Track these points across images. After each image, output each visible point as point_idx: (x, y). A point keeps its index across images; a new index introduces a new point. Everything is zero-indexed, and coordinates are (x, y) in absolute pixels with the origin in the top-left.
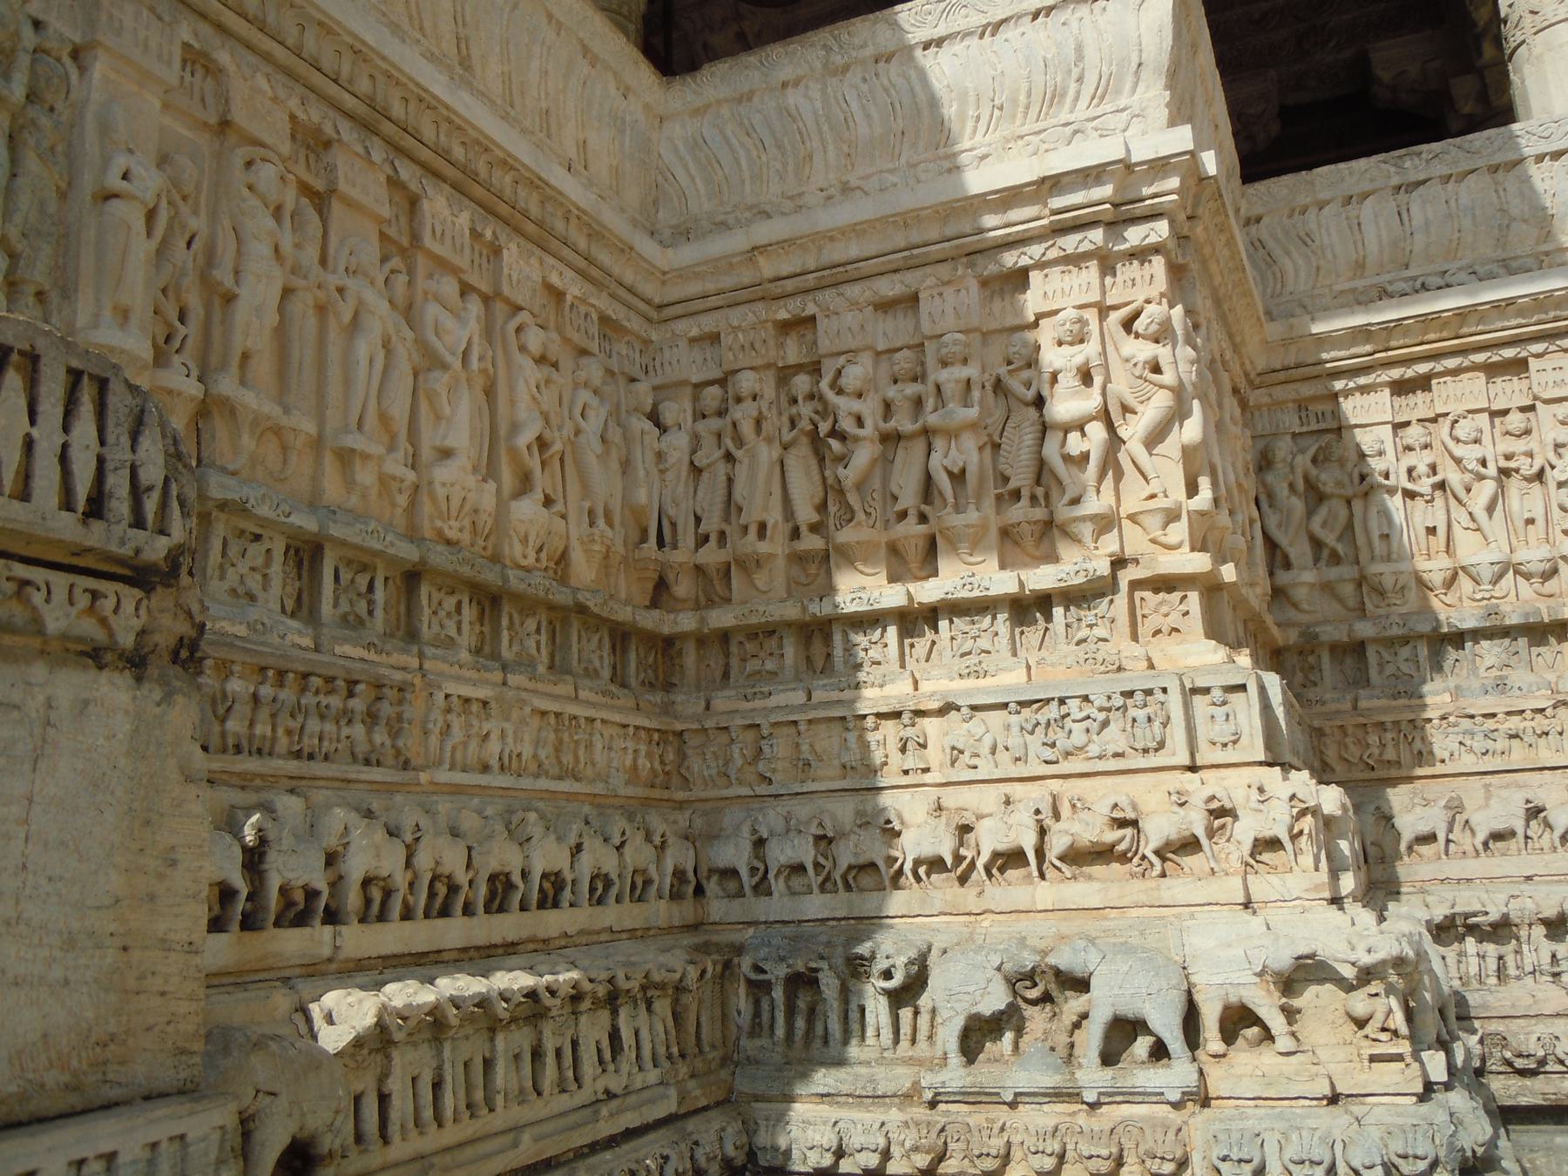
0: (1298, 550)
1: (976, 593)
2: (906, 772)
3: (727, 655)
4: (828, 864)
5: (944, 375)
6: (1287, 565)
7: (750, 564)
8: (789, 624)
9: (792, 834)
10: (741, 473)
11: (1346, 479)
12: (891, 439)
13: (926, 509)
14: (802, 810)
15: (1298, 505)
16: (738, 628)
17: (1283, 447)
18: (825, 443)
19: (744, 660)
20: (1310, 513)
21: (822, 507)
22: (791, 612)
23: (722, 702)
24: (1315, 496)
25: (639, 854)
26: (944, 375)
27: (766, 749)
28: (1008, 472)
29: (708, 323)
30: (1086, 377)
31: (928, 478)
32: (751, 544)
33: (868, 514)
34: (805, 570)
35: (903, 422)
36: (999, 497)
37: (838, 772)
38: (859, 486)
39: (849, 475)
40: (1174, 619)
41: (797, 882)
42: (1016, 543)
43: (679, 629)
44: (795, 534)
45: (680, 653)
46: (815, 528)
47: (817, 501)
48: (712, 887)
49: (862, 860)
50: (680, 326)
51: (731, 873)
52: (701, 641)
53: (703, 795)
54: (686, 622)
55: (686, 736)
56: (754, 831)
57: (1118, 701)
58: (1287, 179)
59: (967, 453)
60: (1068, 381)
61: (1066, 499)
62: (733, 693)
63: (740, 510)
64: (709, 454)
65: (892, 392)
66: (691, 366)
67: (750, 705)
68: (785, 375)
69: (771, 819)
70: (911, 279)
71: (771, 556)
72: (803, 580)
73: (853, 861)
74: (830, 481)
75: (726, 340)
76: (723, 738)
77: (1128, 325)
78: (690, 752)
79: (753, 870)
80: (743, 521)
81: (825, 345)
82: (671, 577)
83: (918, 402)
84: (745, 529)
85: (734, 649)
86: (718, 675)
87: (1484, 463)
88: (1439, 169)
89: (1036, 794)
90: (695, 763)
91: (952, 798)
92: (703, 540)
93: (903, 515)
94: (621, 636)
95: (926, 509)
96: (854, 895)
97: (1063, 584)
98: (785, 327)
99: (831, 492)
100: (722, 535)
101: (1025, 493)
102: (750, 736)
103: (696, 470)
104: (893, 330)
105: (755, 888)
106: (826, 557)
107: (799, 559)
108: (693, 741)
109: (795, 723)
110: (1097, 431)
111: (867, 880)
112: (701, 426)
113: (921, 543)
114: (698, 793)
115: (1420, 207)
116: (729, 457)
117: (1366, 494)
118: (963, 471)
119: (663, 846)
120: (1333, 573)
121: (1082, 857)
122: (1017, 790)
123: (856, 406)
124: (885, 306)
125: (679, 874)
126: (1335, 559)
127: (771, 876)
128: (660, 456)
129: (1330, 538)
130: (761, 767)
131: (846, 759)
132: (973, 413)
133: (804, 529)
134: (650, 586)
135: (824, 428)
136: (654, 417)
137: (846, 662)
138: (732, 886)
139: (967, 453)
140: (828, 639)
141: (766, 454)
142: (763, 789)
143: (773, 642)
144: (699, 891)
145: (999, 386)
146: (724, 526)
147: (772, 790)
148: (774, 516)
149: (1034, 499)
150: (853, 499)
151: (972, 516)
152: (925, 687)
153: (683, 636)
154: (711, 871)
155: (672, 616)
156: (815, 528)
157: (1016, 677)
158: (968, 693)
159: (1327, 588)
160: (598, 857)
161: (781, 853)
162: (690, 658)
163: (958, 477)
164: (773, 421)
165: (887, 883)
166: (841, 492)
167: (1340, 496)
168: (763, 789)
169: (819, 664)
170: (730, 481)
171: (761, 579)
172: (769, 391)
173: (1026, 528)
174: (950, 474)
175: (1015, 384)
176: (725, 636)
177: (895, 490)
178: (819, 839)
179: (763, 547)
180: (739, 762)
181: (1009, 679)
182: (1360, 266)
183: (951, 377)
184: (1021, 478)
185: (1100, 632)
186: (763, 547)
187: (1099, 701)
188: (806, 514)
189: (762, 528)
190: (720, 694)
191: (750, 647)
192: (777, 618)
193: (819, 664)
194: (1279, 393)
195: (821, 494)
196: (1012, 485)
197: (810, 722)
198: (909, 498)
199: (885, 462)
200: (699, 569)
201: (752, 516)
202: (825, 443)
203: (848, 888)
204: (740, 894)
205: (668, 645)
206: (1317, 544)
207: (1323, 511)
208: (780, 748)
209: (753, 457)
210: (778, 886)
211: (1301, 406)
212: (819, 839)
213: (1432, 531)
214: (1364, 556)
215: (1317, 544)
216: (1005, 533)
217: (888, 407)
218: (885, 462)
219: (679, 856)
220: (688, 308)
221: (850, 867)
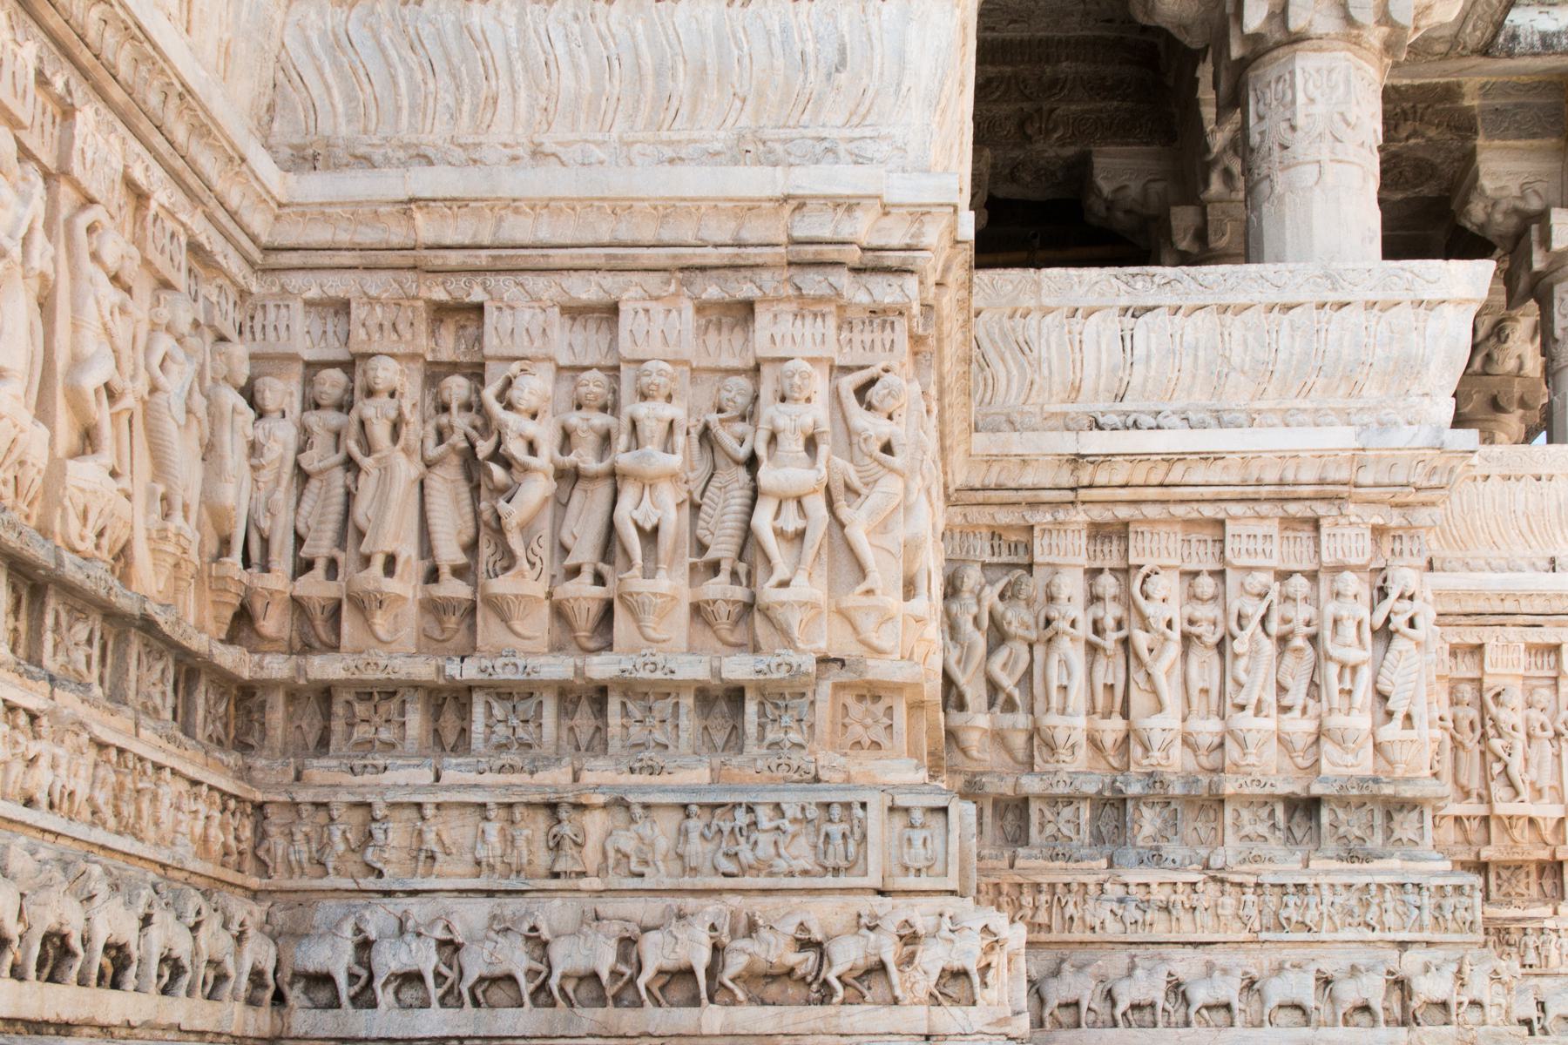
0: (975, 693)
1: (659, 675)
2: (556, 875)
3: (327, 715)
4: (452, 975)
5: (642, 410)
6: (961, 706)
8: (416, 686)
9: (408, 937)
11: (1031, 622)
12: (569, 477)
13: (605, 568)
14: (418, 910)
15: (980, 642)
16: (346, 684)
19: (351, 725)
20: (990, 651)
21: (472, 548)
22: (423, 670)
23: (321, 771)
24: (998, 635)
25: (215, 940)
26: (642, 410)
27: (379, 835)
28: (707, 540)
30: (811, 444)
31: (611, 528)
33: (533, 565)
34: (440, 622)
35: (586, 458)
36: (693, 567)
37: (469, 868)
38: (526, 528)
39: (513, 514)
40: (878, 733)
41: (409, 994)
42: (708, 624)
43: (264, 675)
44: (433, 575)
45: (262, 707)
46: (458, 572)
47: (466, 537)
48: (295, 995)
49: (498, 970)
51: (324, 979)
52: (293, 694)
53: (289, 884)
54: (277, 667)
55: (269, 810)
56: (358, 930)
57: (812, 813)
58: (1015, 274)
59: (665, 509)
60: (793, 445)
61: (774, 580)
62: (334, 763)
63: (361, 535)
65: (574, 419)
67: (358, 780)
69: (378, 920)
71: (400, 598)
72: (437, 634)
73: (485, 972)
74: (487, 515)
76: (322, 817)
77: (861, 391)
78: (273, 830)
79: (353, 978)
80: (364, 549)
82: (258, 606)
83: (606, 439)
84: (366, 561)
85: (339, 709)
86: (312, 739)
87: (1169, 625)
88: (1168, 298)
89: (711, 909)
90: (278, 843)
91: (608, 907)
92: (308, 565)
93: (575, 572)
94: (190, 670)
95: (605, 568)
96: (484, 1012)
97: (761, 677)
99: (488, 532)
100: (332, 566)
101: (726, 567)
102: (358, 816)
104: (585, 344)
105: (354, 1000)
106: (472, 610)
107: (435, 608)
108: (276, 817)
109: (419, 806)
110: (817, 506)
111: (497, 994)
113: (595, 608)
114: (280, 880)
117: (1050, 640)
118: (656, 529)
119: (240, 938)
120: (1007, 720)
121: (767, 982)
122: (690, 903)
123: (531, 428)
125: (257, 977)
126: (1010, 706)
127: (378, 984)
129: (1007, 682)
130: (370, 855)
131: (481, 853)
132: (675, 461)
133: (445, 572)
134: (228, 614)
135: (484, 448)
137: (487, 740)
138: (323, 995)
139: (665, 509)
140: (464, 710)
142: (370, 883)
143: (394, 705)
144: (279, 998)
146: (336, 553)
147: (382, 884)
148: (408, 551)
149: (734, 574)
150: (515, 542)
152: (588, 778)
153: (270, 685)
154: (297, 976)
155: (256, 657)
156: (458, 572)
157: (699, 775)
158: (639, 788)
159: (999, 737)
160: (168, 935)
161: (390, 959)
162: (277, 715)
163: (650, 536)
165: (526, 998)
166: (499, 530)
167: (1024, 639)
168: (370, 883)
169: (450, 737)
171: (381, 622)
173: (723, 609)
174: (640, 529)
176: (326, 693)
177: (568, 540)
178: (441, 944)
179: (392, 586)
180: (341, 847)
181: (693, 775)
183: (652, 414)
184: (723, 547)
185: (794, 737)
186: (392, 586)
187: (791, 811)
188: (449, 552)
189: (390, 563)
190: (315, 762)
191: (360, 709)
192: (402, 675)
193: (450, 737)
195: (471, 531)
196: (711, 555)
197: (438, 806)
198: (585, 552)
199: (561, 504)
201: (380, 543)
202: (482, 468)
203: (476, 1003)
204: (335, 1003)
205: (246, 697)
206: (993, 687)
207: (1002, 655)
208: (395, 835)
210: (385, 997)
212: (441, 944)
213: (1110, 688)
214: (1039, 706)
215: (993, 687)
216: (697, 610)
217: (567, 439)
218: (561, 504)
219: (260, 952)
221: (481, 980)
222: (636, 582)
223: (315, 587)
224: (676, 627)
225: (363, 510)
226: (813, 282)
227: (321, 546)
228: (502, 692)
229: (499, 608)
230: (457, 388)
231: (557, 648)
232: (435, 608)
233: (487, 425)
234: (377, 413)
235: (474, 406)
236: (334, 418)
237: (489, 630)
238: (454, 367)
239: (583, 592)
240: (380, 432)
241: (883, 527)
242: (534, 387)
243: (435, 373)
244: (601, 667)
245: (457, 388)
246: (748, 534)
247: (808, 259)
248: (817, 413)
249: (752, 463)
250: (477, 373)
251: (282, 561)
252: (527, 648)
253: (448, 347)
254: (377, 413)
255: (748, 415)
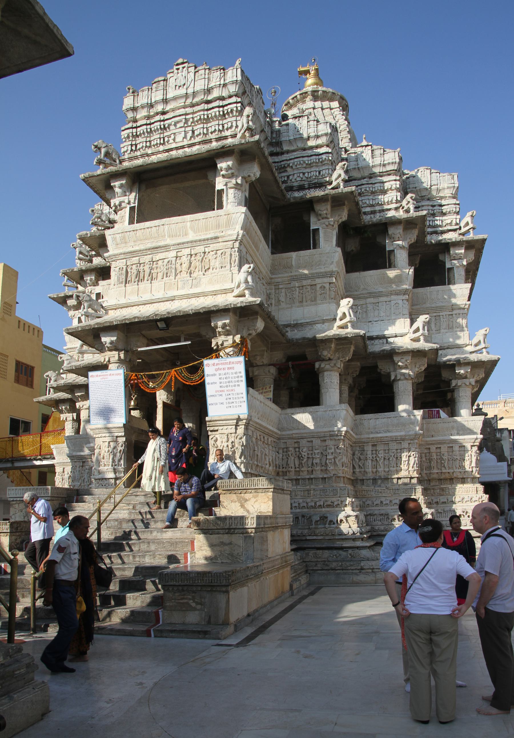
7: (289, 471)
10: (289, 460)
17: (357, 452)
18: (300, 458)
21: (299, 465)
29: (285, 441)
30: (332, 453)
32: (290, 469)
39: (303, 462)
44: (295, 468)
50: (281, 441)
59: (318, 461)
64: (284, 457)
65: (309, 452)
66: (282, 446)
68: (295, 448)
70: (312, 439)
75: (288, 443)
77: (337, 448)
81: (301, 446)
83: (312, 454)
92: (283, 468)
98: (295, 442)
99: (301, 464)
103: (283, 459)
104: (310, 444)
110: (333, 460)
112: (284, 454)
115: (378, 422)
116: (287, 458)
124: (308, 441)
128: (278, 457)
136: (278, 452)
139: (318, 461)
141: (293, 458)
145: (322, 453)
148: (293, 466)
151: (318, 468)
163: (316, 464)
164: (294, 454)
166: (302, 463)
170: (287, 461)
171: (291, 473)
172: (293, 450)
175: (324, 453)
182: (369, 428)
184: (323, 464)
188: (297, 466)
189: (292, 467)
194: (357, 445)
198: (310, 465)
200: (283, 471)
201: (290, 466)
209: (291, 459)
211: (360, 446)
216: (321, 470)
217: (308, 454)
218: (307, 460)
220: (283, 439)
222: (315, 468)
223: (284, 470)
224: (319, 472)
225: (289, 462)
226: (332, 438)
227: (284, 466)
228: (303, 479)
229: (302, 471)
230: (297, 449)
231: (307, 474)
232: (295, 471)
233: (300, 453)
234: (290, 453)
235: (299, 451)
236: (286, 453)
237: (301, 473)
238: (296, 448)
239: (310, 469)
240: (290, 455)
241: (339, 460)
242: (304, 450)
243: (295, 448)
244: (312, 476)
245: (297, 449)
246: (326, 463)
247: (331, 436)
248: (333, 450)
249: (326, 456)
250: (299, 448)
251: (281, 468)
252: (305, 475)
253: (296, 445)
254: (290, 453)
255: (326, 450)
